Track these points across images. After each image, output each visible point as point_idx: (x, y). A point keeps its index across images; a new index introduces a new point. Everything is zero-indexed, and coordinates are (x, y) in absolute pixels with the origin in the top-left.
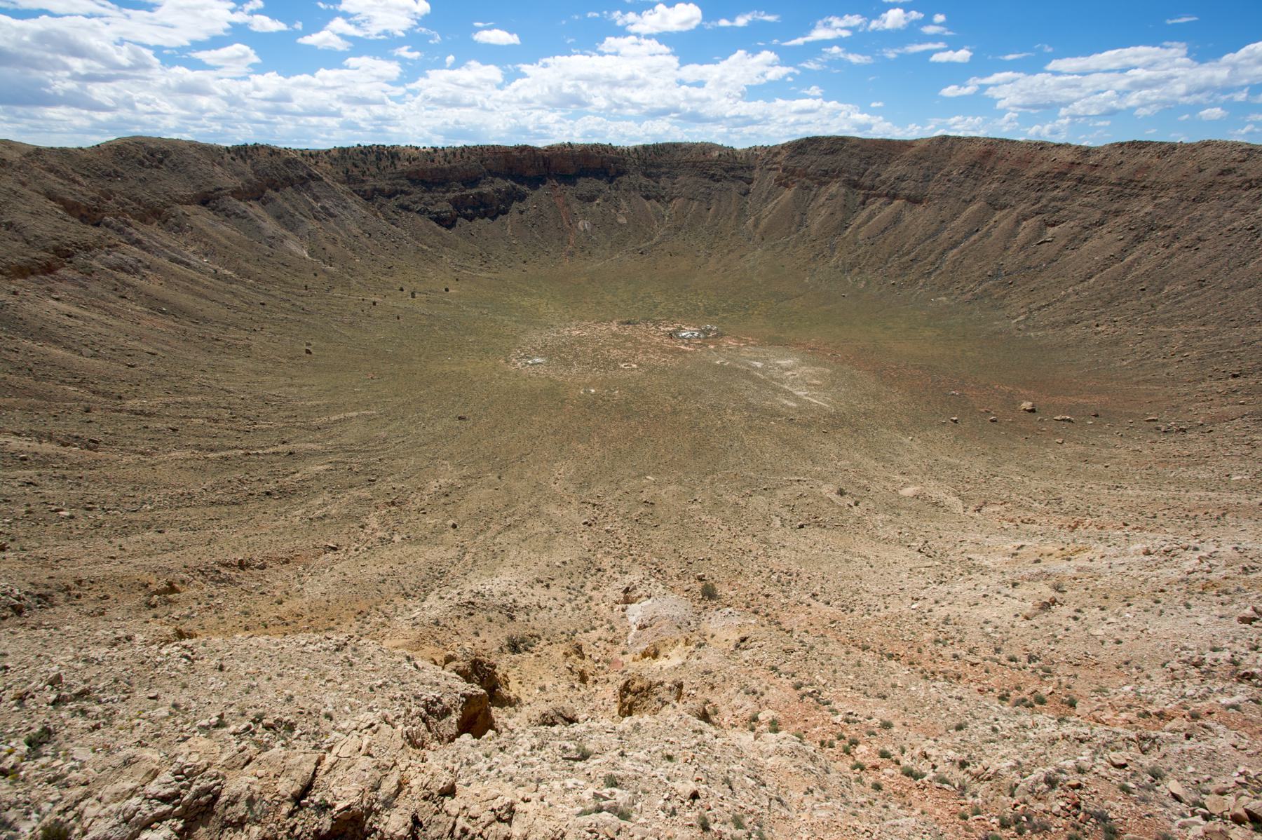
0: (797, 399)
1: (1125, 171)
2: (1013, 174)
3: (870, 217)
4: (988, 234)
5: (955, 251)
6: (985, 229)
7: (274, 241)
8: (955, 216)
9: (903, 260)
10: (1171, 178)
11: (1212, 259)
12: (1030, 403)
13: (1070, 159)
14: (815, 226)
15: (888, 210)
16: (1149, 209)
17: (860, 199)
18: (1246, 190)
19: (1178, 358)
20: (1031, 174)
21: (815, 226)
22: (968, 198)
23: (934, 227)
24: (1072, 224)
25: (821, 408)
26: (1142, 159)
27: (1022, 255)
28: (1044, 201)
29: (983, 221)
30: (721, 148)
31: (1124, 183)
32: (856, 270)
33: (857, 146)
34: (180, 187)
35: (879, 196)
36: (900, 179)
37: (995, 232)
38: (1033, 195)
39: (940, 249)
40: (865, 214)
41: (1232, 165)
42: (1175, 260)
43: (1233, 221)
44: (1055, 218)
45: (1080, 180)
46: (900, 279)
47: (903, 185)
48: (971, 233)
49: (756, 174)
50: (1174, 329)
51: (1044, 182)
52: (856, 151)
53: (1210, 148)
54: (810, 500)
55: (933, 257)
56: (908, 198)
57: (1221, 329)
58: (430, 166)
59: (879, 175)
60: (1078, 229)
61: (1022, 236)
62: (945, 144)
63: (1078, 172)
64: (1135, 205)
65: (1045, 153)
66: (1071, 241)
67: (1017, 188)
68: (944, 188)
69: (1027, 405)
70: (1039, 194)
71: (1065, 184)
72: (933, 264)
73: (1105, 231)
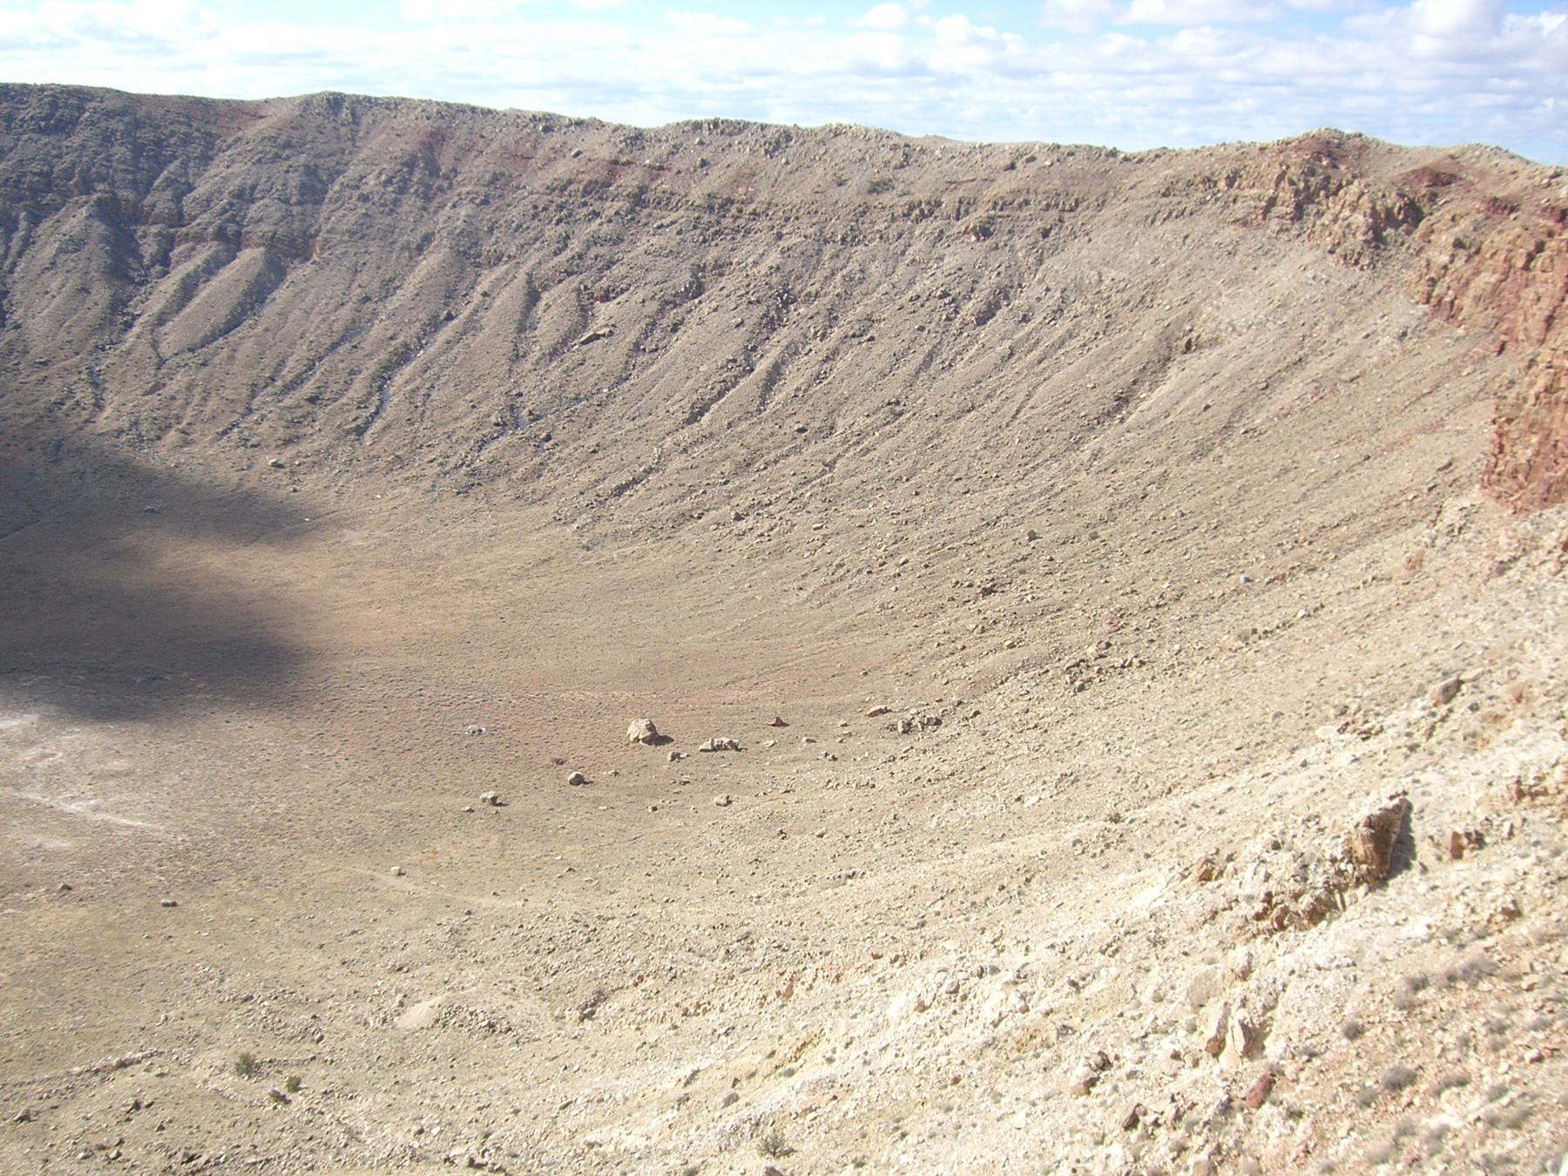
0: (72, 825)
1: (714, 181)
3: (187, 290)
5: (408, 370)
6: (466, 312)
8: (389, 287)
9: (288, 401)
10: (795, 197)
11: (898, 358)
12: (643, 723)
13: (606, 153)
15: (226, 274)
16: (773, 258)
17: (149, 249)
18: (917, 221)
19: (891, 569)
20: (537, 185)
22: (415, 239)
23: (346, 313)
24: (641, 294)
25: (142, 837)
26: (740, 157)
27: (555, 372)
28: (575, 246)
31: (718, 205)
32: (172, 436)
33: (122, 113)
35: (199, 238)
36: (244, 196)
37: (489, 319)
38: (552, 232)
39: (371, 367)
40: (169, 286)
41: (887, 174)
42: (840, 364)
43: (911, 283)
44: (604, 283)
45: (638, 199)
46: (290, 451)
47: (253, 211)
48: (435, 324)
50: (870, 509)
51: (569, 201)
52: (117, 125)
53: (841, 141)
54: (164, 1114)
55: (358, 389)
56: (271, 242)
57: (946, 498)
59: (191, 188)
60: (653, 306)
62: (340, 114)
63: (629, 181)
64: (746, 251)
65: (555, 139)
66: (647, 333)
67: (514, 214)
68: (352, 218)
69: (637, 728)
70: (561, 228)
71: (610, 208)
72: (362, 404)
73: (705, 308)
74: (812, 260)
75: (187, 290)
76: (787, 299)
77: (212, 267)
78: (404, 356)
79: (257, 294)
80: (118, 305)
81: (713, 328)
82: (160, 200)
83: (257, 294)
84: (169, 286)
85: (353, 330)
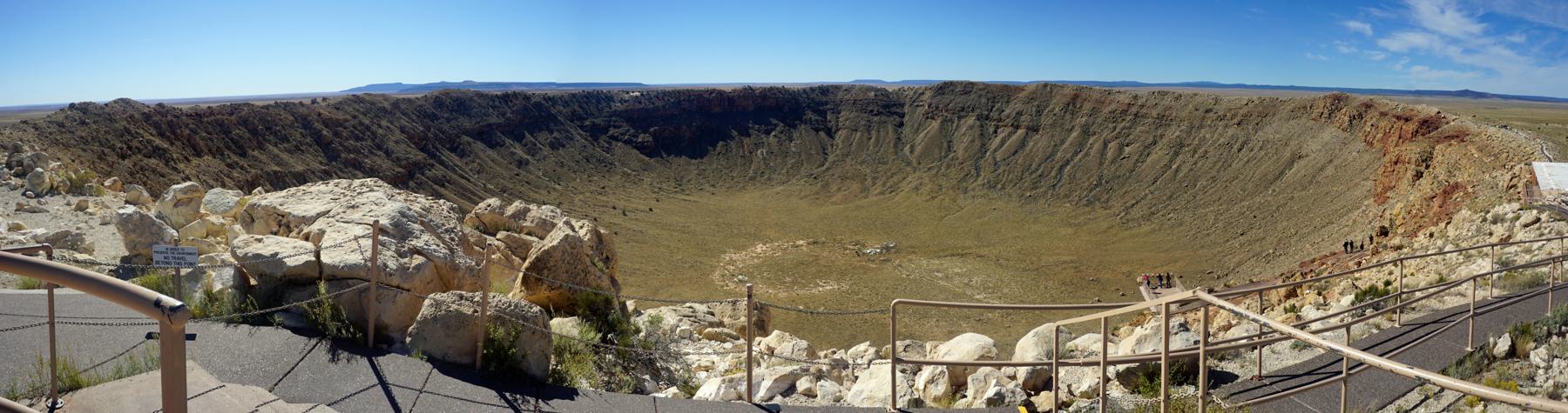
2: (1094, 111)
4: (1087, 154)
7: (521, 163)
8: (1063, 142)
14: (960, 153)
15: (1014, 137)
17: (991, 130)
21: (960, 153)
29: (1081, 145)
30: (877, 90)
34: (466, 123)
37: (1093, 152)
40: (998, 140)
48: (1076, 153)
49: (906, 109)
56: (1028, 128)
58: (638, 106)
61: (1110, 154)
74: (1189, 133)
75: (1003, 142)
76: (1182, 146)
77: (1010, 135)
78: (1067, 163)
79: (1023, 144)
80: (983, 145)
81: (1158, 155)
82: (994, 115)
83: (1023, 144)
84: (998, 140)
85: (1053, 154)
